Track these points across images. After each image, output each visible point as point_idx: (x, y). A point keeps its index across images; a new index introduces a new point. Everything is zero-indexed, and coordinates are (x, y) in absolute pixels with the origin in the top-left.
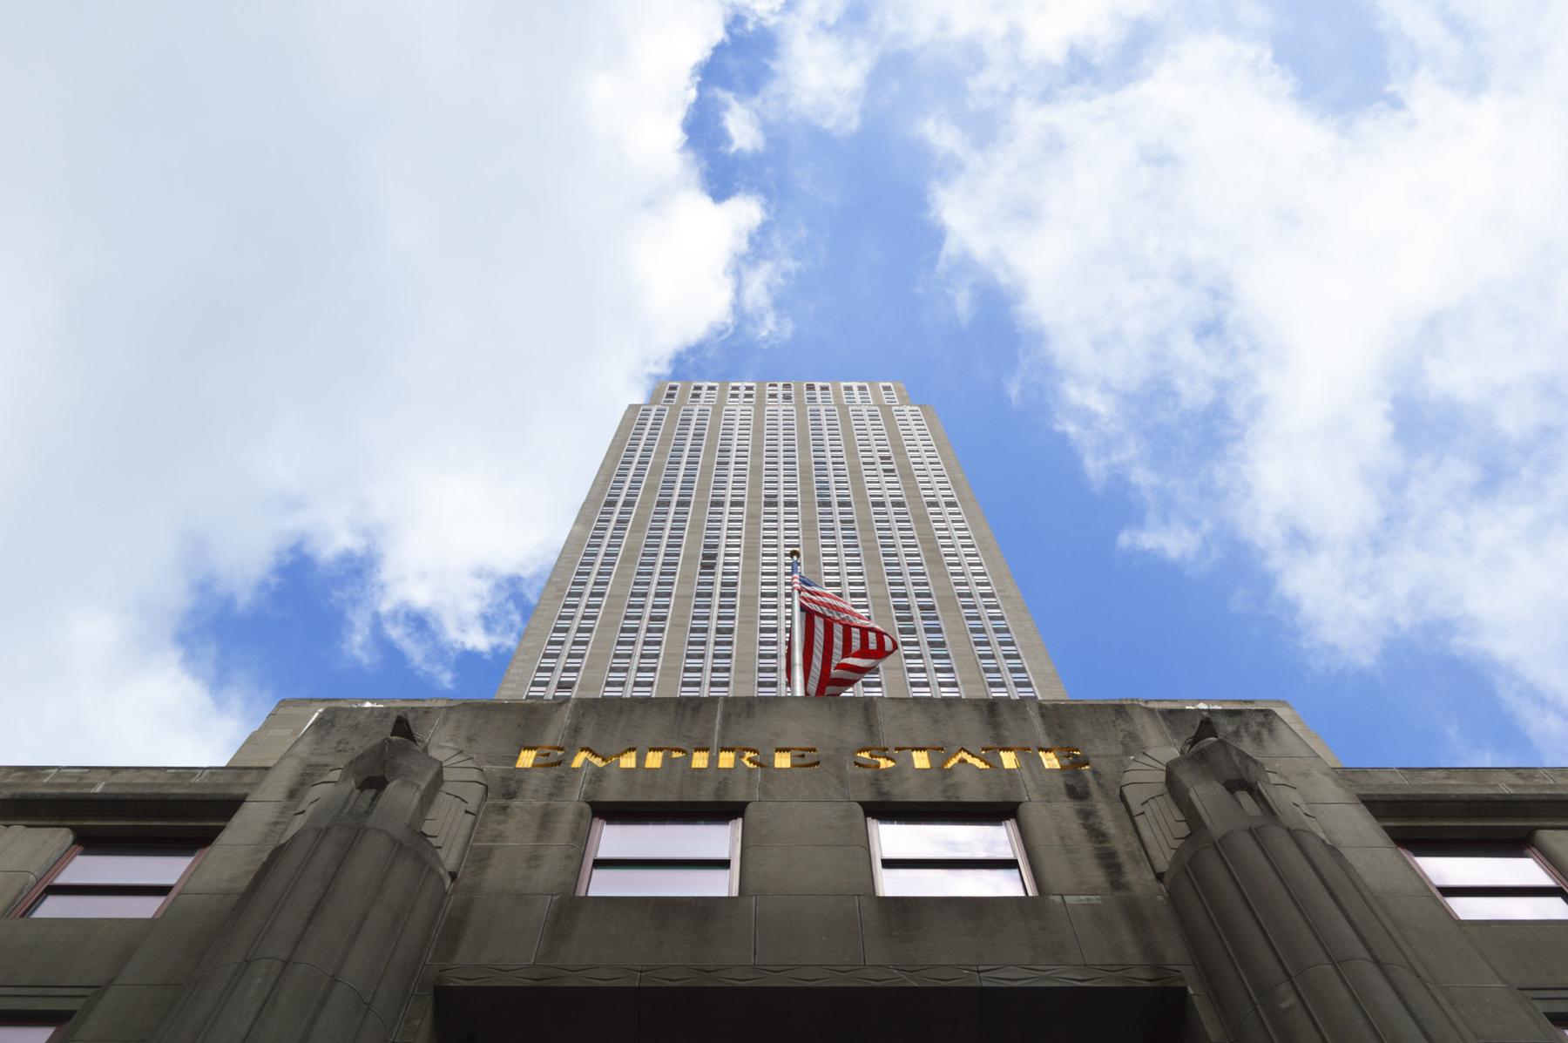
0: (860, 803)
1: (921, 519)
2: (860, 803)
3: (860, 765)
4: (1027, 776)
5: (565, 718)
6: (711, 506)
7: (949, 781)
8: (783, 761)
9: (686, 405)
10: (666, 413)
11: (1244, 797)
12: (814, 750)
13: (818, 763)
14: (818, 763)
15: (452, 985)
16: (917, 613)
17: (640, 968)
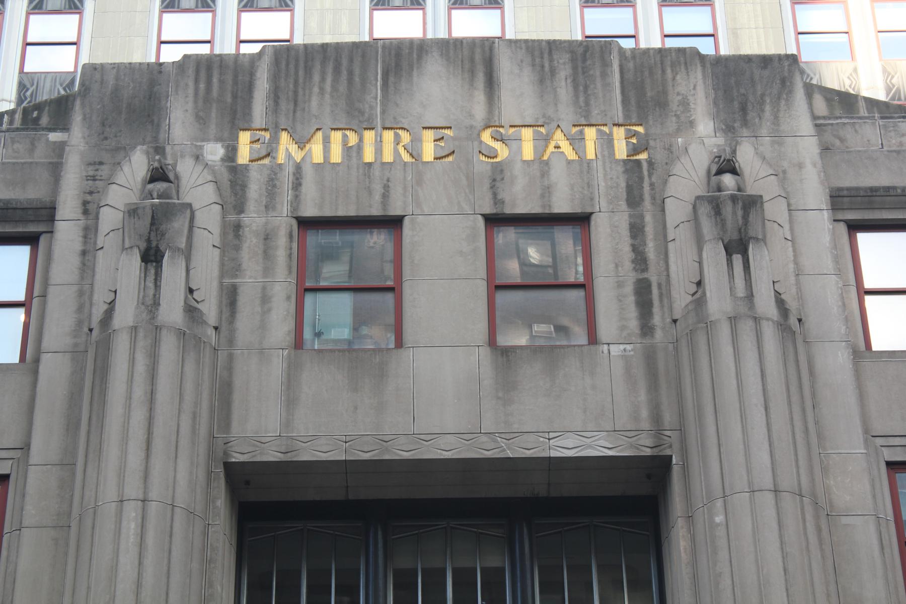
11: (737, 259)
13: (453, 152)
15: (234, 460)
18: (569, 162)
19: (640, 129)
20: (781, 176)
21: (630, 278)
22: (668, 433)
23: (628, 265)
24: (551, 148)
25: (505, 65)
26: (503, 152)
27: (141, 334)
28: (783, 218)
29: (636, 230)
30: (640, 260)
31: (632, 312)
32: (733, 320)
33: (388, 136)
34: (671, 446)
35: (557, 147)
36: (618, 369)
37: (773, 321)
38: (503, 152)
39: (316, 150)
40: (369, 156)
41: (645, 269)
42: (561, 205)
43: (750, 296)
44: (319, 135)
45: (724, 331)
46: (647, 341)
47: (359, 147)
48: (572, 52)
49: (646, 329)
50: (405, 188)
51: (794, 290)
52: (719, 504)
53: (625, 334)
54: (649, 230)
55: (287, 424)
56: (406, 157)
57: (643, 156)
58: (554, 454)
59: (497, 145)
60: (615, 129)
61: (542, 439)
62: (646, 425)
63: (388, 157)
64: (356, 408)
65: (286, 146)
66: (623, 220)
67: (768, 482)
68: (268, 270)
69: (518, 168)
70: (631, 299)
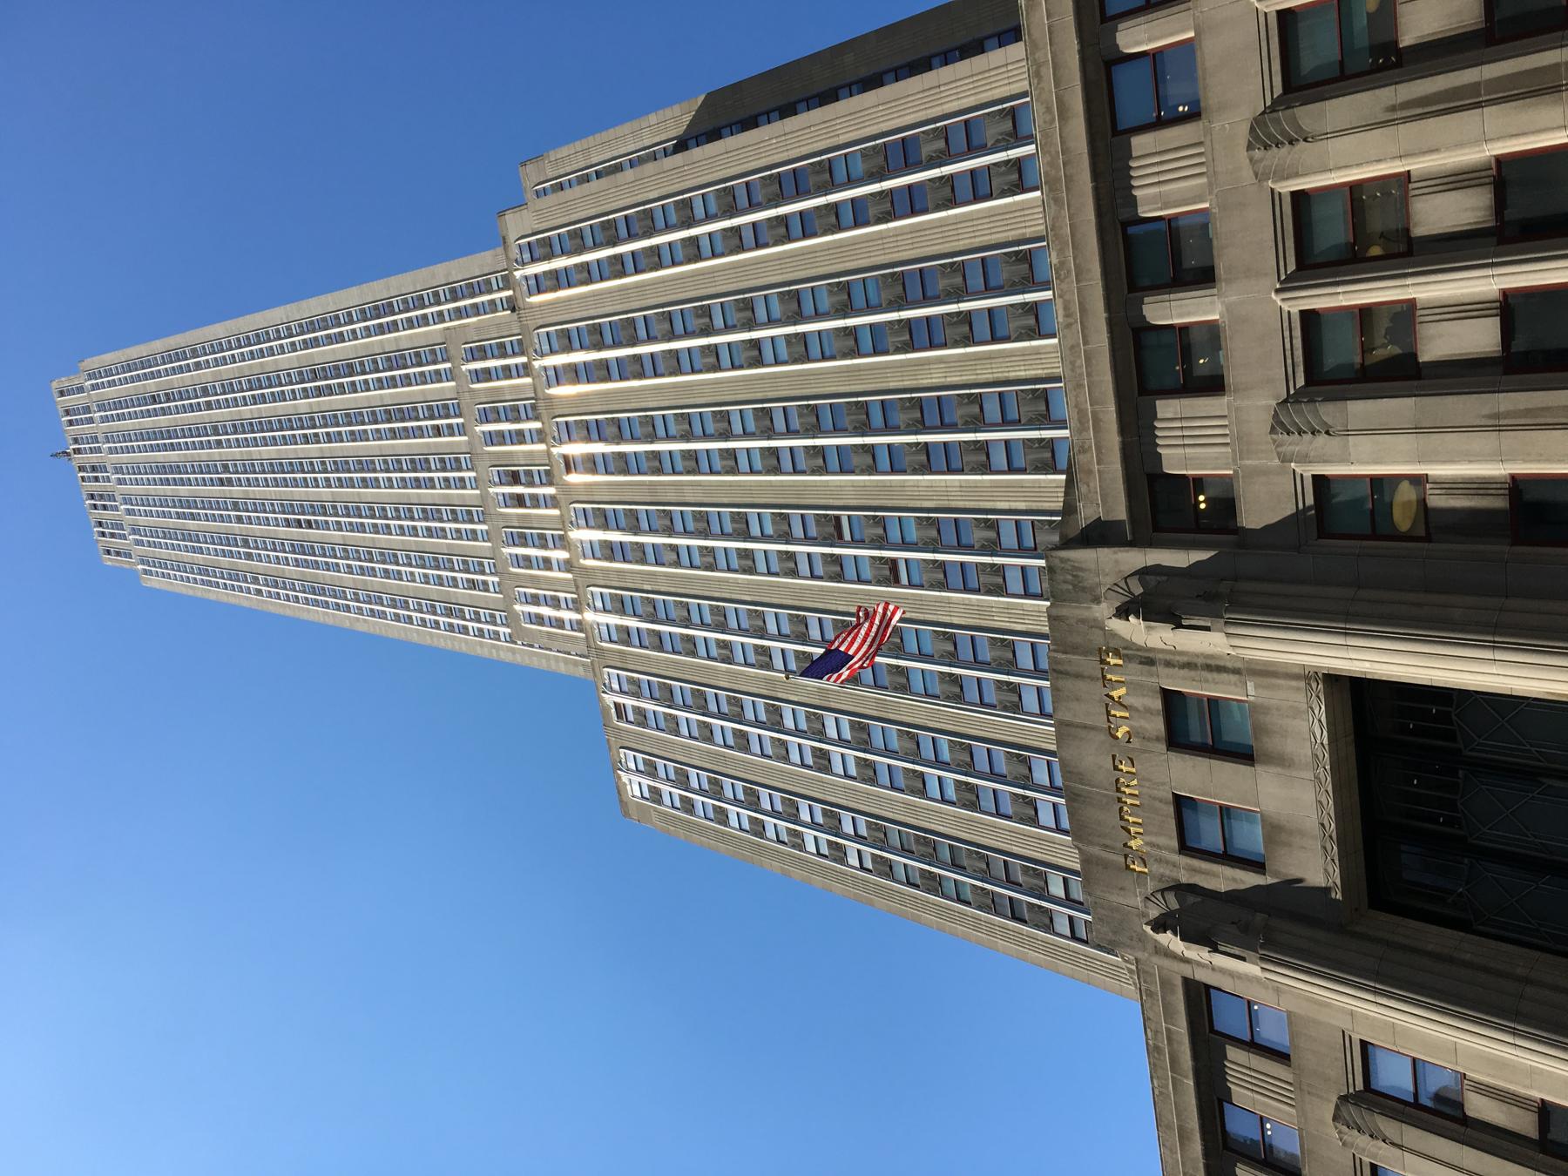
18: (1127, 694)
22: (1307, 672)
23: (1193, 673)
29: (1168, 664)
31: (1224, 676)
34: (1316, 673)
36: (1265, 693)
41: (1196, 665)
42: (1157, 704)
46: (1244, 672)
48: (1057, 678)
54: (1168, 657)
58: (1326, 742)
66: (1162, 670)
68: (1215, 875)
70: (1215, 675)
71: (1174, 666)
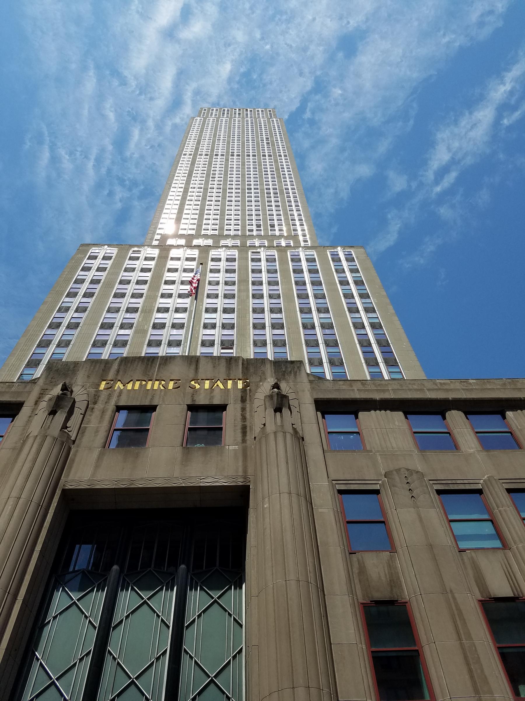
0: (187, 405)
1: (276, 161)
2: (187, 405)
3: (191, 387)
4: (232, 391)
5: (115, 366)
6: (215, 156)
7: (212, 395)
8: (171, 385)
9: (208, 117)
10: (202, 120)
12: (180, 380)
13: (179, 387)
14: (179, 387)
15: (67, 488)
16: (272, 195)
17: (116, 480)
19: (248, 381)
20: (296, 392)
21: (239, 424)
22: (249, 477)
24: (216, 385)
25: (202, 362)
26: (198, 386)
27: (38, 438)
28: (297, 406)
30: (244, 418)
32: (275, 433)
33: (157, 383)
34: (250, 482)
35: (218, 385)
37: (291, 434)
38: (198, 386)
39: (129, 386)
40: (149, 387)
43: (282, 426)
44: (132, 382)
45: (272, 437)
46: (244, 445)
47: (146, 385)
49: (244, 441)
50: (160, 397)
51: (300, 427)
52: (267, 500)
53: (235, 442)
55: (93, 475)
56: (162, 388)
57: (249, 388)
58: (201, 485)
59: (197, 385)
60: (239, 381)
61: (198, 479)
62: (241, 473)
63: (156, 387)
64: (123, 469)
65: (119, 385)
67: (286, 490)
69: (202, 391)
71: (242, 411)
